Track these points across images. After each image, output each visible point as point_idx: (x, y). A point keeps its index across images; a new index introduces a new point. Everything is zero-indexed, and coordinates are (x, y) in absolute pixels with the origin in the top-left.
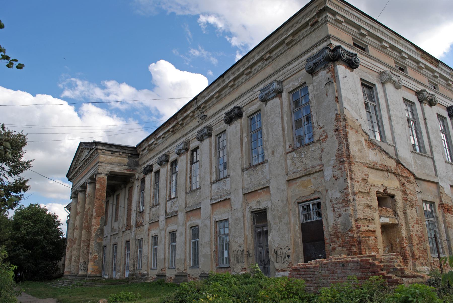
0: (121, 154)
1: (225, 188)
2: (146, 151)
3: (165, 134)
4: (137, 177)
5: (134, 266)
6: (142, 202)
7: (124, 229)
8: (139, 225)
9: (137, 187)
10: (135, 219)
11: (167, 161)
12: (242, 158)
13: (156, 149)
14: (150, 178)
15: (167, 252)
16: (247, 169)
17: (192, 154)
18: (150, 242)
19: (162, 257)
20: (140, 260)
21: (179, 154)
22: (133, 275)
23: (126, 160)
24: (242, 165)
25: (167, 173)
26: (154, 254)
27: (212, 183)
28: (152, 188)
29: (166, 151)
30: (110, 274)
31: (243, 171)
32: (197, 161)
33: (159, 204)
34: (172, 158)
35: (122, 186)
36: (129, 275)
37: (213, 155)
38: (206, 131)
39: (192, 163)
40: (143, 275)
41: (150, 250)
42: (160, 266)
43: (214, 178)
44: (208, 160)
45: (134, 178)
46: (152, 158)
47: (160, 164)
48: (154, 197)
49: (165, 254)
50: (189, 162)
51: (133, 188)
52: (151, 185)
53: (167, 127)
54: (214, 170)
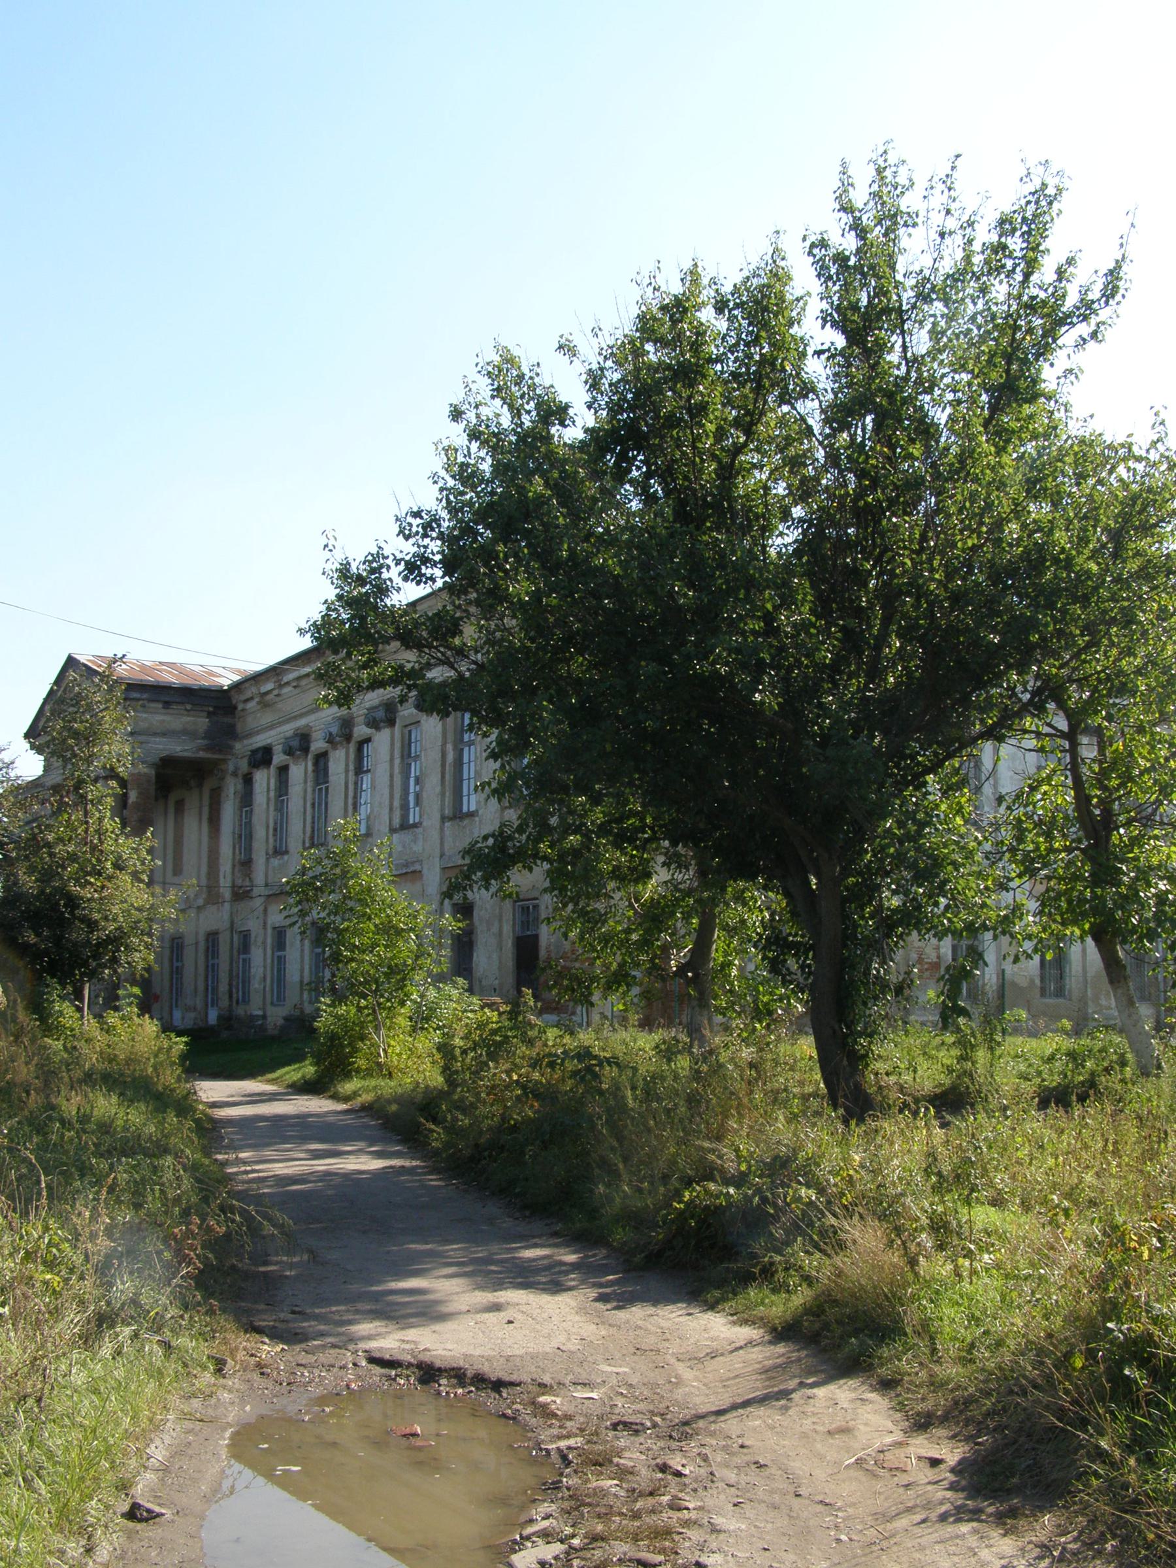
0: (189, 707)
1: (415, 848)
2: (251, 705)
3: (299, 678)
4: (231, 768)
5: (231, 996)
6: (245, 837)
7: (200, 902)
8: (241, 895)
9: (231, 796)
10: (229, 879)
11: (306, 750)
12: (443, 794)
13: (279, 706)
14: (263, 780)
15: (307, 967)
16: (450, 819)
17: (359, 750)
18: (269, 941)
19: (296, 978)
20: (246, 982)
21: (330, 740)
22: (230, 1018)
23: (201, 722)
24: (442, 809)
25: (305, 782)
26: (279, 971)
27: (393, 830)
28: (272, 808)
29: (302, 722)
30: (166, 1015)
31: (443, 819)
32: (368, 771)
33: (287, 852)
34: (318, 745)
35: (193, 783)
36: (220, 1017)
37: (397, 770)
38: (380, 714)
39: (360, 770)
40: (252, 1018)
41: (269, 961)
42: (292, 996)
43: (397, 822)
44: (386, 779)
45: (223, 767)
46: (271, 727)
47: (289, 752)
48: (275, 830)
49: (302, 970)
50: (352, 767)
51: (223, 795)
52: (268, 799)
53: (304, 666)
54: (397, 803)
